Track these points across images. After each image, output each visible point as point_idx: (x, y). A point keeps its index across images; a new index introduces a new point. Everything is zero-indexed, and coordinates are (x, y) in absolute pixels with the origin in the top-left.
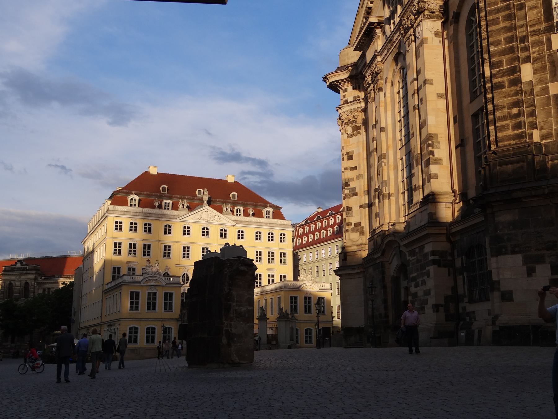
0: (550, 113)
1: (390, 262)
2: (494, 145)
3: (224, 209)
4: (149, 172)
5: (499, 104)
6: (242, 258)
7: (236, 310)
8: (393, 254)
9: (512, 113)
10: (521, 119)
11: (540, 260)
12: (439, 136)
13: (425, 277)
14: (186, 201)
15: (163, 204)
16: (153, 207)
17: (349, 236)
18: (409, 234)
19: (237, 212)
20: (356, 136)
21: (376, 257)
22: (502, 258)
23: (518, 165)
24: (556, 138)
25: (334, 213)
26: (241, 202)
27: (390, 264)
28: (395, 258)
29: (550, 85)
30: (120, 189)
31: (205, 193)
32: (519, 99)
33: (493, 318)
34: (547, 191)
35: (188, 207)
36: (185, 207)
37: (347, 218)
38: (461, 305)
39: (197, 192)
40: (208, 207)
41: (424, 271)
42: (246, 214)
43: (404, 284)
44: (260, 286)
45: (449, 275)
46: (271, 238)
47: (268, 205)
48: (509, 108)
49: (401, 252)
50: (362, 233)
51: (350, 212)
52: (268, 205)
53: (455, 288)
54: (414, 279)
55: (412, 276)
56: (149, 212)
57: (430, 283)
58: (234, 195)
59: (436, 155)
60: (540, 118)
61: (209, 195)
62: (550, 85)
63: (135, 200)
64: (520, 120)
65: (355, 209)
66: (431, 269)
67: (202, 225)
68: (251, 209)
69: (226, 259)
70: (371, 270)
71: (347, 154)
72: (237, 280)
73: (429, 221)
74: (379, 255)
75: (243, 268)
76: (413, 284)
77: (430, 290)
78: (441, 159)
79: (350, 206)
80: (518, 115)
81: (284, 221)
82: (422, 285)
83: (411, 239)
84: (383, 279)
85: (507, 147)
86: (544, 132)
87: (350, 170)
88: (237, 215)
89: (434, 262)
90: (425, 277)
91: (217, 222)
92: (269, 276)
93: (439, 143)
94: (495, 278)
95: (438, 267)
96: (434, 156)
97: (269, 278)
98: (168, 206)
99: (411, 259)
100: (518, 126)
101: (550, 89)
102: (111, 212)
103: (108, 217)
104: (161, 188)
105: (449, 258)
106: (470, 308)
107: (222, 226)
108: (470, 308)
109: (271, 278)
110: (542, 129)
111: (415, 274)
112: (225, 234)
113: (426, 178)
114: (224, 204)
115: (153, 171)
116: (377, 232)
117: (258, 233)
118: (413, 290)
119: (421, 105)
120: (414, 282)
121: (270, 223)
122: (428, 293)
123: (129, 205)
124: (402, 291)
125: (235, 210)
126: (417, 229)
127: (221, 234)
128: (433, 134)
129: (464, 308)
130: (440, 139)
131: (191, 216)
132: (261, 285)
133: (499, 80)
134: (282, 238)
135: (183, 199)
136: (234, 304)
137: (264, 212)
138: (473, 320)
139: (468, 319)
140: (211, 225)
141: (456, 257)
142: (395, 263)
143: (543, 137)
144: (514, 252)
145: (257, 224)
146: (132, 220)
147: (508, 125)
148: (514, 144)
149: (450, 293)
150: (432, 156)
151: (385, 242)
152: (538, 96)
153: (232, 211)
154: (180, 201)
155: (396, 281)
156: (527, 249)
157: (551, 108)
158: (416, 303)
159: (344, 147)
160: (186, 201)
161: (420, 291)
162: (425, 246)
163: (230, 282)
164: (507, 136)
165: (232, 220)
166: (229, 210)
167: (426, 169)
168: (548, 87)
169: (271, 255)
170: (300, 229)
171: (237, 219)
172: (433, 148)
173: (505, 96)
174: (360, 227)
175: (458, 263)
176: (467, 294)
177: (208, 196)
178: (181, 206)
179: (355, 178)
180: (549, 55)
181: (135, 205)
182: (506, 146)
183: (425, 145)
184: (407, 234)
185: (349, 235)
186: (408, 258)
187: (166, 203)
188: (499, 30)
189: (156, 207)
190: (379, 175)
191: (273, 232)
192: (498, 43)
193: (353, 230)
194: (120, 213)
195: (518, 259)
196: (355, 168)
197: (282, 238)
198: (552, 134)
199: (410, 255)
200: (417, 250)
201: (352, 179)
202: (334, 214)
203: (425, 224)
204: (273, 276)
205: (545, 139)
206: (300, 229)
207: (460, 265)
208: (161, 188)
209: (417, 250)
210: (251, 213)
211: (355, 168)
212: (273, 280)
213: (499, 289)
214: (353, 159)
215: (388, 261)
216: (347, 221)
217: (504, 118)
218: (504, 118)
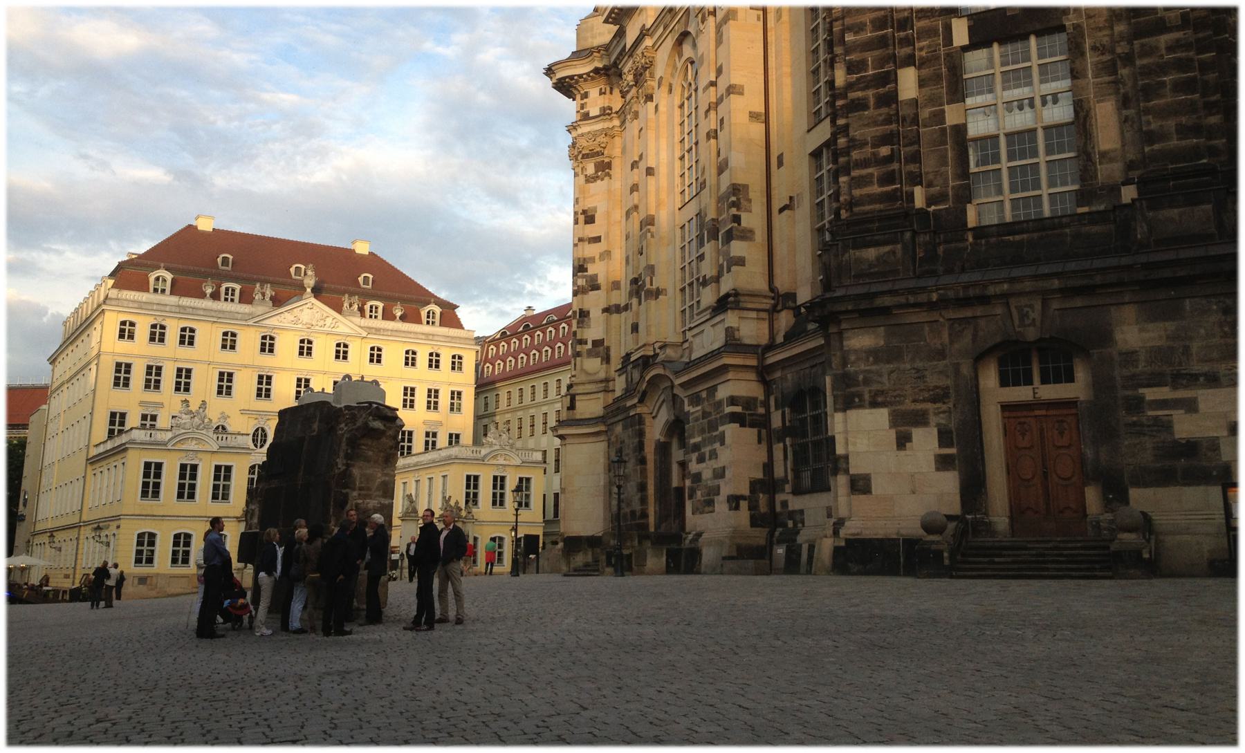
0: (946, 157)
1: (654, 415)
2: (847, 211)
3: (346, 305)
4: (196, 228)
5: (857, 138)
6: (375, 406)
7: (357, 505)
8: (661, 399)
9: (879, 154)
10: (895, 166)
11: (920, 419)
12: (750, 189)
13: (717, 445)
14: (269, 285)
15: (223, 289)
16: (202, 295)
17: (582, 366)
18: (691, 364)
19: (371, 311)
20: (602, 180)
21: (629, 404)
22: (853, 414)
23: (887, 249)
24: (953, 203)
25: (556, 318)
26: (379, 293)
27: (653, 418)
28: (664, 408)
29: (946, 107)
30: (134, 256)
31: (309, 273)
32: (891, 131)
33: (834, 524)
34: (935, 297)
35: (272, 298)
36: (267, 299)
37: (579, 331)
38: (780, 497)
39: (292, 270)
40: (313, 300)
41: (715, 434)
42: (388, 316)
43: (677, 454)
44: (408, 453)
45: (760, 442)
46: (434, 362)
47: (432, 300)
48: (875, 146)
49: (674, 396)
50: (607, 359)
51: (586, 319)
52: (432, 300)
53: (768, 467)
54: (696, 447)
55: (692, 441)
56: (192, 305)
57: (725, 456)
58: (365, 279)
59: (744, 224)
60: (929, 164)
61: (316, 276)
62: (946, 107)
63: (164, 280)
64: (892, 168)
65: (596, 314)
66: (730, 430)
67: (297, 333)
68: (399, 306)
69: (342, 405)
70: (619, 429)
71: (584, 212)
72: (363, 447)
73: (726, 341)
74: (635, 400)
75: (377, 424)
76: (694, 456)
77: (724, 467)
78: (751, 231)
79: (586, 308)
80: (889, 159)
81: (462, 331)
82: (710, 459)
83: (694, 374)
84: (641, 447)
85: (869, 215)
86: (935, 190)
87: (589, 243)
88: (371, 317)
89: (734, 418)
90: (717, 445)
91: (330, 329)
92: (427, 434)
93: (750, 201)
94: (840, 450)
95: (741, 426)
96: (739, 224)
97: (427, 439)
98: (233, 295)
99: (692, 410)
100: (888, 179)
101: (946, 114)
102: (113, 303)
103: (107, 313)
104: (219, 260)
105: (761, 410)
106: (795, 503)
107: (339, 338)
108: (795, 503)
109: (431, 439)
110: (930, 185)
111: (698, 439)
112: (345, 352)
113: (725, 263)
114: (347, 296)
115: (205, 225)
116: (632, 359)
117: (410, 353)
118: (694, 467)
120: (697, 454)
121: (433, 335)
122: (720, 474)
123: (151, 289)
124: (675, 468)
125: (367, 308)
126: (706, 355)
127: (338, 352)
128: (739, 185)
129: (785, 504)
130: (751, 195)
131: (278, 317)
132: (410, 453)
134: (457, 363)
135: (263, 282)
136: (355, 494)
137: (424, 313)
138: (800, 525)
139: (790, 524)
140: (316, 335)
141: (773, 409)
142: (664, 416)
143: (930, 201)
144: (874, 404)
145: (410, 336)
146: (155, 319)
147: (872, 175)
148: (881, 211)
149: (759, 475)
150: (736, 225)
151: (647, 379)
152: (925, 126)
153: (361, 310)
154: (258, 285)
155: (663, 450)
156: (898, 399)
157: (946, 150)
158: (699, 493)
159: (580, 200)
160: (269, 285)
161: (706, 469)
162: (719, 386)
163: (349, 451)
164: (869, 196)
165: (360, 327)
166: (355, 307)
167: (725, 248)
168: (943, 111)
169: (433, 394)
170: (492, 347)
171: (370, 325)
172: (738, 209)
173: (869, 123)
174: (601, 348)
175: (776, 421)
176: (789, 478)
177: (314, 278)
178: (258, 297)
179: (597, 257)
181: (163, 291)
182: (867, 213)
184: (688, 363)
185: (582, 362)
186: (687, 408)
187: (227, 289)
189: (208, 295)
190: (641, 254)
191: (439, 352)
193: (590, 354)
194: (131, 305)
195: (882, 415)
196: (597, 239)
197: (457, 363)
198: (948, 195)
199: (692, 403)
200: (704, 395)
201: (592, 260)
202: (556, 321)
203: (719, 349)
204: (435, 435)
205: (936, 204)
206: (492, 347)
207: (780, 424)
208: (219, 260)
209: (704, 395)
210: (399, 314)
211: (597, 239)
212: (434, 443)
213: (847, 471)
214: (594, 222)
215: (651, 413)
216: (579, 337)
217: (864, 164)
218: (864, 164)
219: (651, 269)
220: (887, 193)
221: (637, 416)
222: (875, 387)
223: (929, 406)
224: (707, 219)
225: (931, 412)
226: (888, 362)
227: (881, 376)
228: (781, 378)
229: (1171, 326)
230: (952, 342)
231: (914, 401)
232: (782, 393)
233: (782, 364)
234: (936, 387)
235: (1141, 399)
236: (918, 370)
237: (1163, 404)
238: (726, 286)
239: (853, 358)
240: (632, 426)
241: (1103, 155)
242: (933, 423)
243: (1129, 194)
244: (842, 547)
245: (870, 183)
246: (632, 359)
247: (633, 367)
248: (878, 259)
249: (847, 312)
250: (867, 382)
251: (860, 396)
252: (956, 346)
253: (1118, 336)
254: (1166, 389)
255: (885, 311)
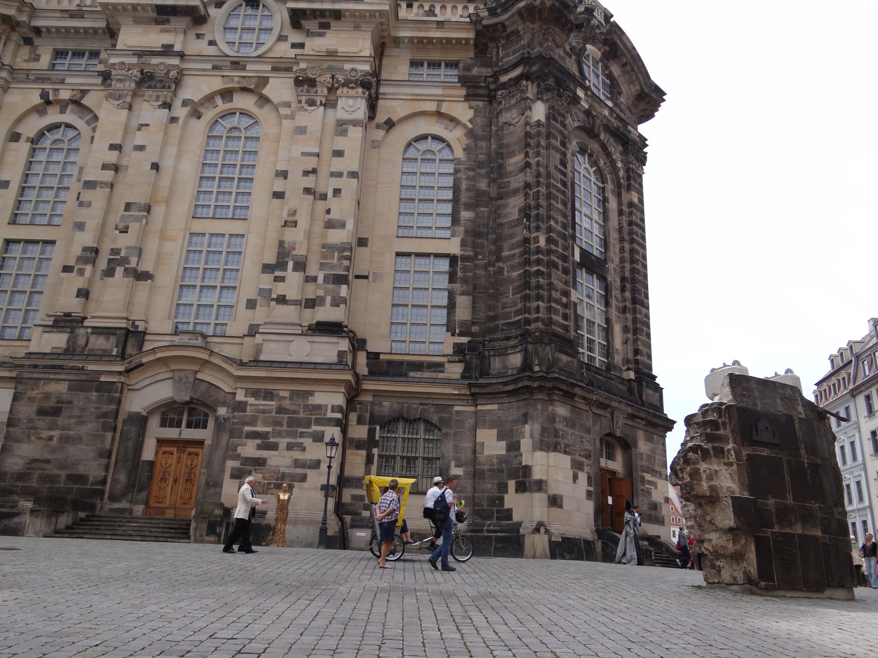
22: (552, 455)
23: (570, 359)
119: (334, 196)
133: (555, 259)
144: (566, 453)
167: (331, 286)
180: (573, 262)
183: (336, 254)
188: (558, 210)
192: (557, 222)
213: (546, 491)
219: (140, 252)
220: (564, 325)
221: (120, 385)
222: (566, 441)
223: (583, 459)
224: (294, 253)
225: (585, 464)
226: (571, 428)
227: (568, 435)
228: (372, 403)
229: (651, 445)
230: (594, 426)
231: (580, 455)
232: (372, 414)
233: (376, 393)
234: (587, 450)
235: (644, 478)
236: (581, 438)
237: (650, 483)
238: (326, 313)
239: (558, 419)
240: (97, 391)
241: (616, 350)
242: (586, 471)
243: (632, 375)
244: (559, 542)
245: (558, 314)
246: (85, 324)
247: (92, 333)
248: (567, 362)
249: (560, 390)
250: (563, 437)
251: (560, 445)
252: (595, 428)
253: (639, 444)
254: (650, 475)
255: (573, 395)
